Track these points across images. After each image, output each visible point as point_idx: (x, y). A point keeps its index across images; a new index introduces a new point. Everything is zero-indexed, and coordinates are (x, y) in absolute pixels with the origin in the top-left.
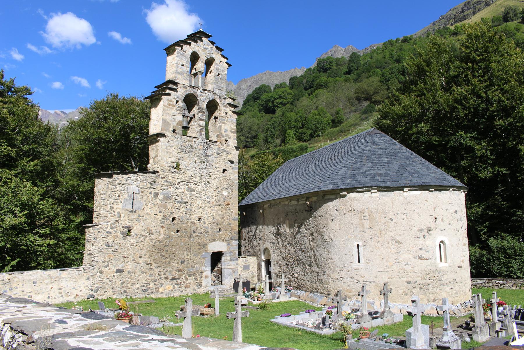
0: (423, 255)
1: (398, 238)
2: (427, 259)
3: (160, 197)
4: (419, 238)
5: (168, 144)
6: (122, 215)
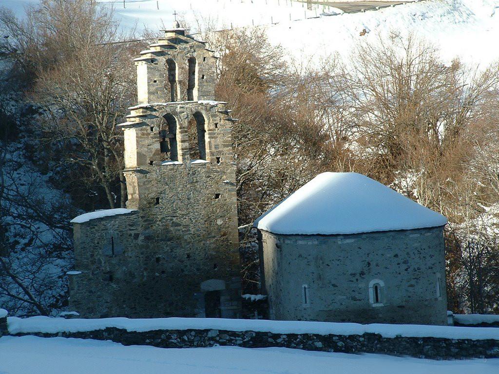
0: (356, 297)
1: (334, 282)
2: (360, 300)
3: (141, 238)
4: (352, 281)
5: (146, 180)
6: (103, 262)
